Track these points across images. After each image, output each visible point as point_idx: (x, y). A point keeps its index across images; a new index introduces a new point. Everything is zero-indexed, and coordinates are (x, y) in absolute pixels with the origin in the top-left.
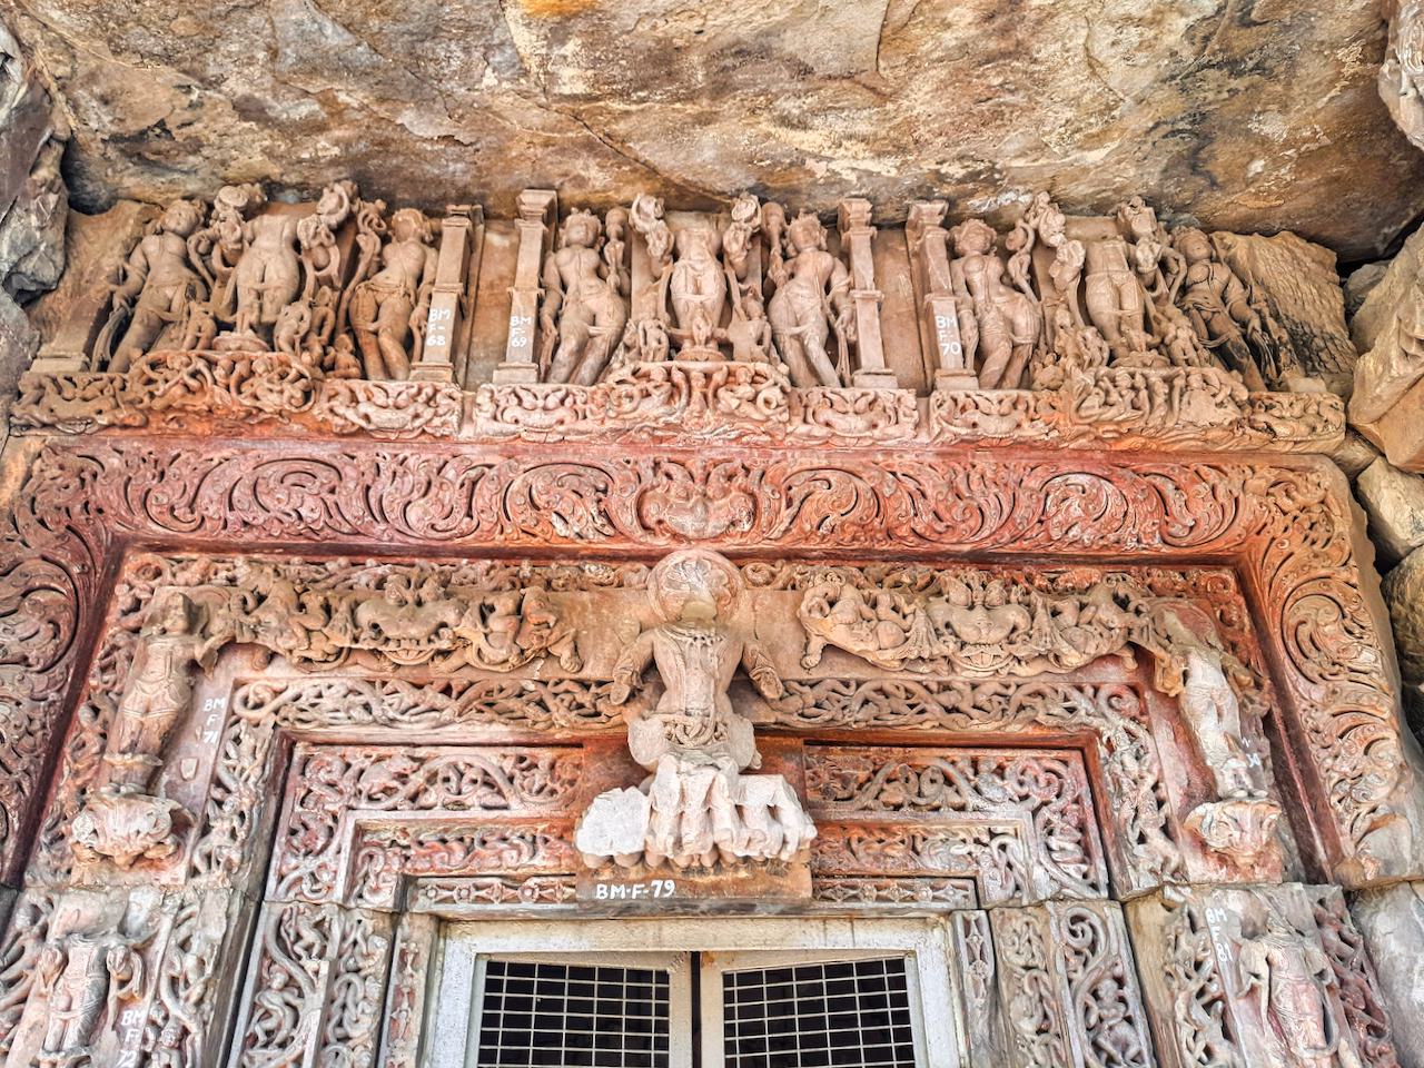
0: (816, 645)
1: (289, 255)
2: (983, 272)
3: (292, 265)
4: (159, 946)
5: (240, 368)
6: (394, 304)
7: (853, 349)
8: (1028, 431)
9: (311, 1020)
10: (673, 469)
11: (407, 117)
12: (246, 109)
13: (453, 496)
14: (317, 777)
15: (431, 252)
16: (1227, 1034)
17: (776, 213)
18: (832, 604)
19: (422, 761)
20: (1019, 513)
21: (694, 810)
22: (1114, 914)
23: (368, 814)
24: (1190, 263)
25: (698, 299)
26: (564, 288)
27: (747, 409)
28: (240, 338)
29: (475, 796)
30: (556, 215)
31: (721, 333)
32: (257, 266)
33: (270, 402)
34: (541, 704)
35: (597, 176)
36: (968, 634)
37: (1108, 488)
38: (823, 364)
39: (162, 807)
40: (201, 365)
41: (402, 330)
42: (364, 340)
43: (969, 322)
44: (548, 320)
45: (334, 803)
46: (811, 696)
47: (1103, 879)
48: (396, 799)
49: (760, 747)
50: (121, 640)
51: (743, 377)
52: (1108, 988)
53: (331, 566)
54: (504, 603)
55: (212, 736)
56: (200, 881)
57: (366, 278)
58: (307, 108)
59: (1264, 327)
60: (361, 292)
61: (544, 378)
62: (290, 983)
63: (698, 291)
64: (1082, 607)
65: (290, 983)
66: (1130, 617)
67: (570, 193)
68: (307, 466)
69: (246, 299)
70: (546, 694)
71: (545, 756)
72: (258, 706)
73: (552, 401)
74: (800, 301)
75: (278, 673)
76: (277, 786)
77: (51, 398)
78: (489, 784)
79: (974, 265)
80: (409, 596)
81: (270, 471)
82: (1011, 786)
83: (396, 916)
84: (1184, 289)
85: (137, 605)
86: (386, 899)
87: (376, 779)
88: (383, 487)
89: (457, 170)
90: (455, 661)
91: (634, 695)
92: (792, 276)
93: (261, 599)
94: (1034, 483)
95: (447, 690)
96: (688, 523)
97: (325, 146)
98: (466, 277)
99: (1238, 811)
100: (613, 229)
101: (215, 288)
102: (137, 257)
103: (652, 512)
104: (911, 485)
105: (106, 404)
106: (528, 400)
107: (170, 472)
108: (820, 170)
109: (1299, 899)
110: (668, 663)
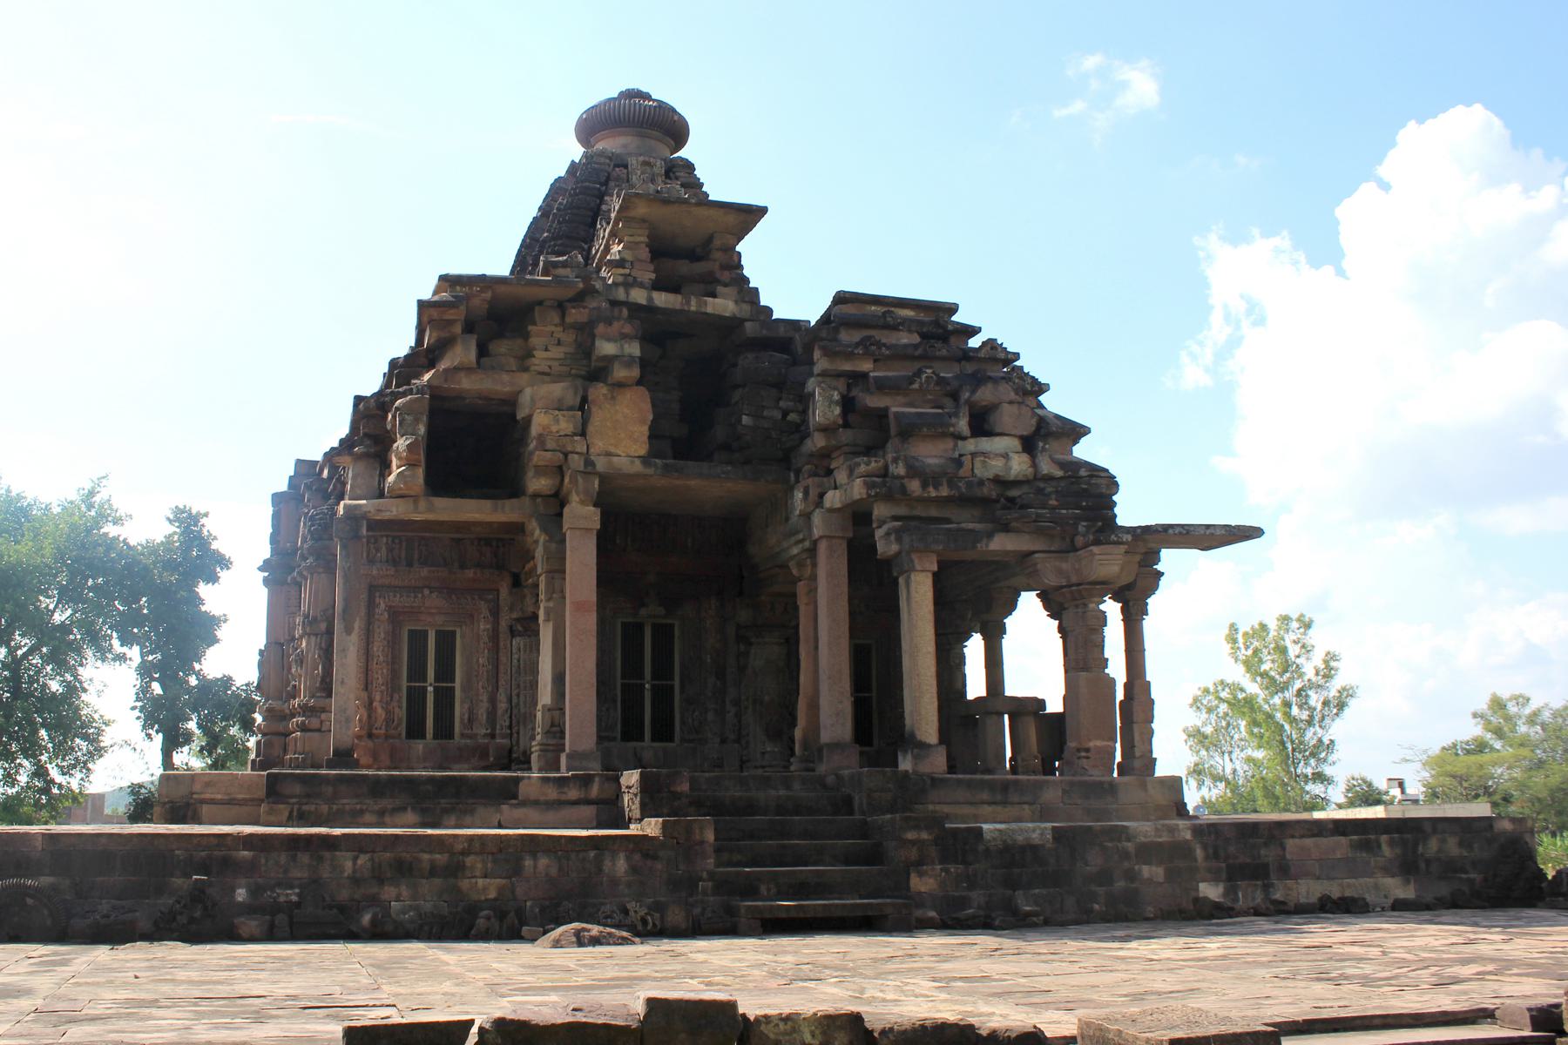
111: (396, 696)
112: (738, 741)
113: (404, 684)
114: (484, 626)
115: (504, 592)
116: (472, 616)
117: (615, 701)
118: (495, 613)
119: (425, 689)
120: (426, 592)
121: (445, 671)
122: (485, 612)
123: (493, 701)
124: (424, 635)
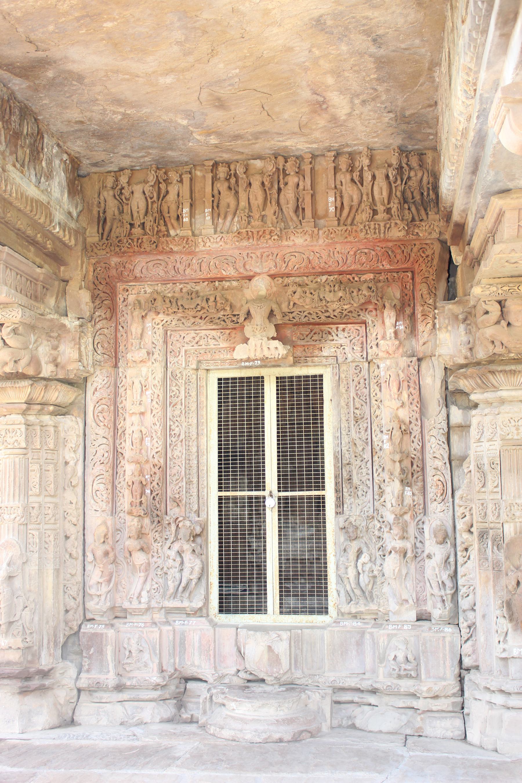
0: (292, 304)
1: (143, 197)
2: (344, 178)
3: (144, 200)
4: (150, 379)
5: (140, 241)
6: (173, 207)
7: (303, 209)
8: (349, 239)
9: (183, 392)
10: (253, 255)
11: (169, 153)
12: (125, 156)
13: (196, 267)
14: (173, 339)
15: (180, 185)
16: (380, 390)
17: (281, 160)
18: (294, 293)
19: (198, 334)
20: (348, 262)
21: (259, 349)
22: (366, 364)
23: (188, 347)
24: (411, 169)
25: (256, 203)
26: (220, 193)
27: (269, 241)
28: (137, 231)
29: (212, 342)
30: (216, 165)
31: (263, 213)
32: (136, 203)
33: (148, 249)
34: (224, 321)
35: (226, 156)
36: (328, 299)
37: (373, 253)
38: (295, 218)
39: (144, 351)
40: (130, 241)
41: (176, 216)
42: (167, 219)
43: (338, 199)
44: (215, 208)
45: (178, 345)
46: (291, 316)
47: (365, 356)
48: (193, 344)
49: (277, 331)
50: (124, 309)
51: (267, 232)
52: (362, 381)
53: (168, 286)
54: (212, 299)
55: (150, 333)
56: (155, 365)
57: (164, 197)
58: (141, 155)
59: (428, 195)
60: (163, 204)
61: (215, 232)
62: (177, 385)
63: (256, 199)
64: (359, 290)
65: (177, 385)
66: (370, 293)
67: (218, 159)
68: (159, 262)
69: (135, 215)
70: (225, 318)
71: (228, 331)
72: (158, 324)
73: (218, 239)
74: (288, 194)
75: (161, 316)
76: (166, 342)
77: (95, 250)
78: (214, 339)
79: (342, 176)
80: (189, 297)
81: (150, 264)
82: (346, 335)
83: (197, 370)
84: (409, 178)
85: (124, 301)
86: (194, 366)
87: (187, 339)
88: (178, 265)
89: (186, 159)
90: (202, 312)
91: (245, 319)
92: (286, 184)
93: (155, 300)
94: (352, 253)
95: (201, 318)
96: (258, 270)
97: (147, 159)
98: (191, 198)
99: (387, 342)
100: (232, 172)
101: (125, 207)
102: (102, 197)
103: (247, 267)
104: (318, 255)
105: (108, 250)
106: (212, 240)
107: (127, 266)
108: (294, 148)
109: (404, 361)
110: (252, 312)
112: (453, 620)
117: (198, 536)
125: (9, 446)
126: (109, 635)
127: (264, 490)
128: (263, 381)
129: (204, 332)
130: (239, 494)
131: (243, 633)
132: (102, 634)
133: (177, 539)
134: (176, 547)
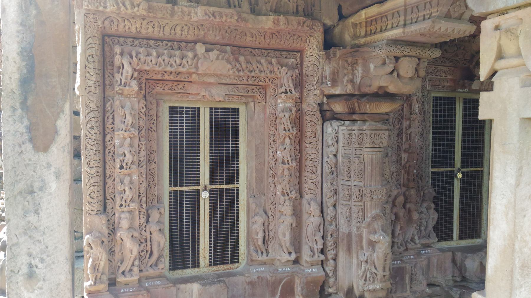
29: (444, 75)
78: (445, 72)
111: (155, 215)
113: (166, 189)
114: (283, 104)
115: (313, 49)
116: (264, 88)
118: (300, 83)
119: (196, 195)
120: (200, 49)
121: (226, 166)
122: (287, 83)
123: (297, 213)
124: (194, 113)
125: (376, 146)
126: (408, 267)
127: (454, 167)
128: (455, 101)
129: (440, 67)
130: (442, 169)
131: (459, 255)
132: (403, 267)
133: (423, 201)
134: (425, 205)
